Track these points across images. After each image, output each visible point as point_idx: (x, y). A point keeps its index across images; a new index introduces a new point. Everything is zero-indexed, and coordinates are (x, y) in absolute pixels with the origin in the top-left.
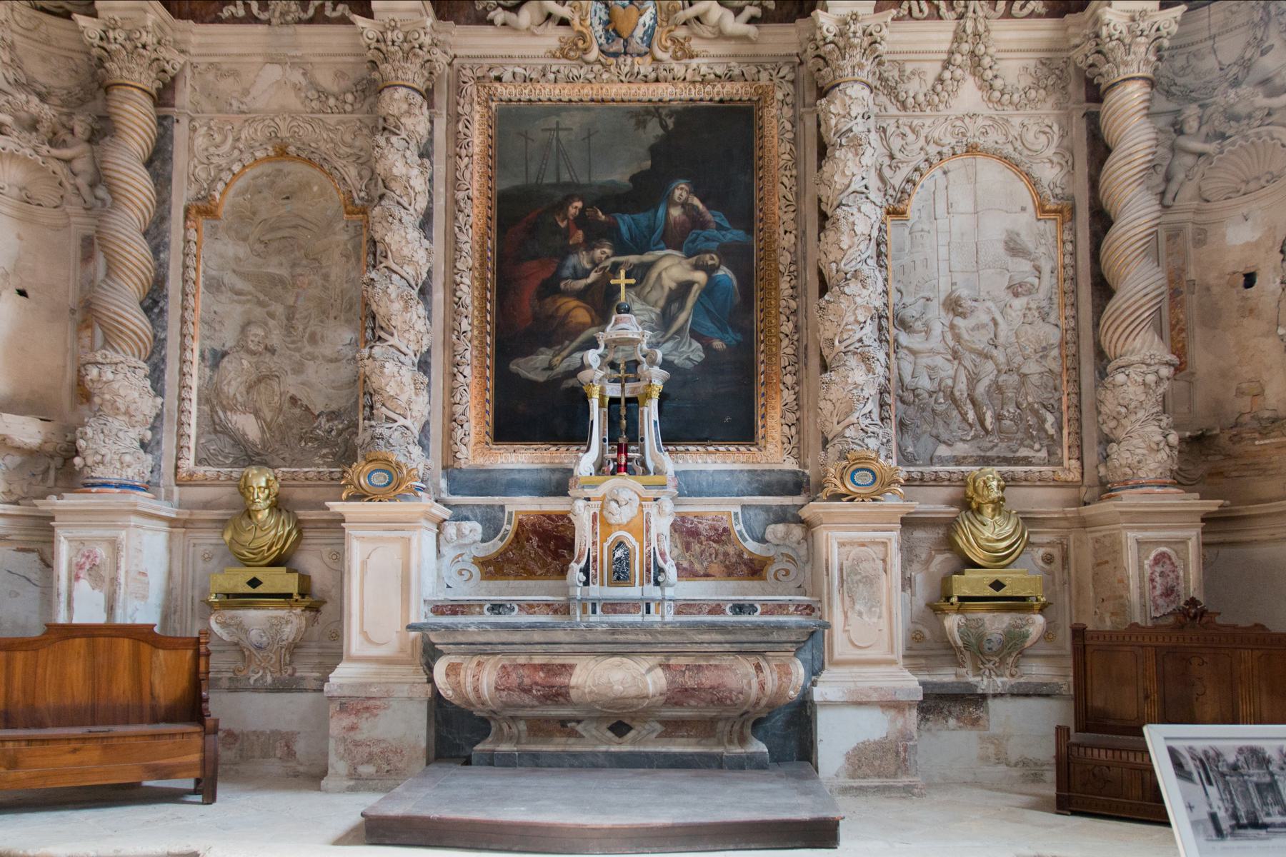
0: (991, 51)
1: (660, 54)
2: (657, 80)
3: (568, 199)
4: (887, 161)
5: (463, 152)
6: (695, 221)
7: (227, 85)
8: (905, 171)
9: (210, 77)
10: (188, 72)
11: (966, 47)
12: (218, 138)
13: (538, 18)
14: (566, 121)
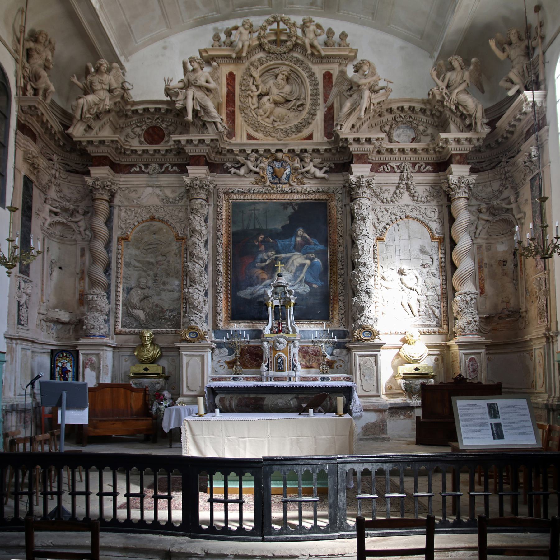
0: (414, 183)
1: (292, 183)
2: (291, 192)
3: (259, 234)
4: (377, 221)
5: (220, 218)
8: (383, 224)
10: (119, 191)
11: (404, 182)
13: (247, 171)
14: (258, 207)
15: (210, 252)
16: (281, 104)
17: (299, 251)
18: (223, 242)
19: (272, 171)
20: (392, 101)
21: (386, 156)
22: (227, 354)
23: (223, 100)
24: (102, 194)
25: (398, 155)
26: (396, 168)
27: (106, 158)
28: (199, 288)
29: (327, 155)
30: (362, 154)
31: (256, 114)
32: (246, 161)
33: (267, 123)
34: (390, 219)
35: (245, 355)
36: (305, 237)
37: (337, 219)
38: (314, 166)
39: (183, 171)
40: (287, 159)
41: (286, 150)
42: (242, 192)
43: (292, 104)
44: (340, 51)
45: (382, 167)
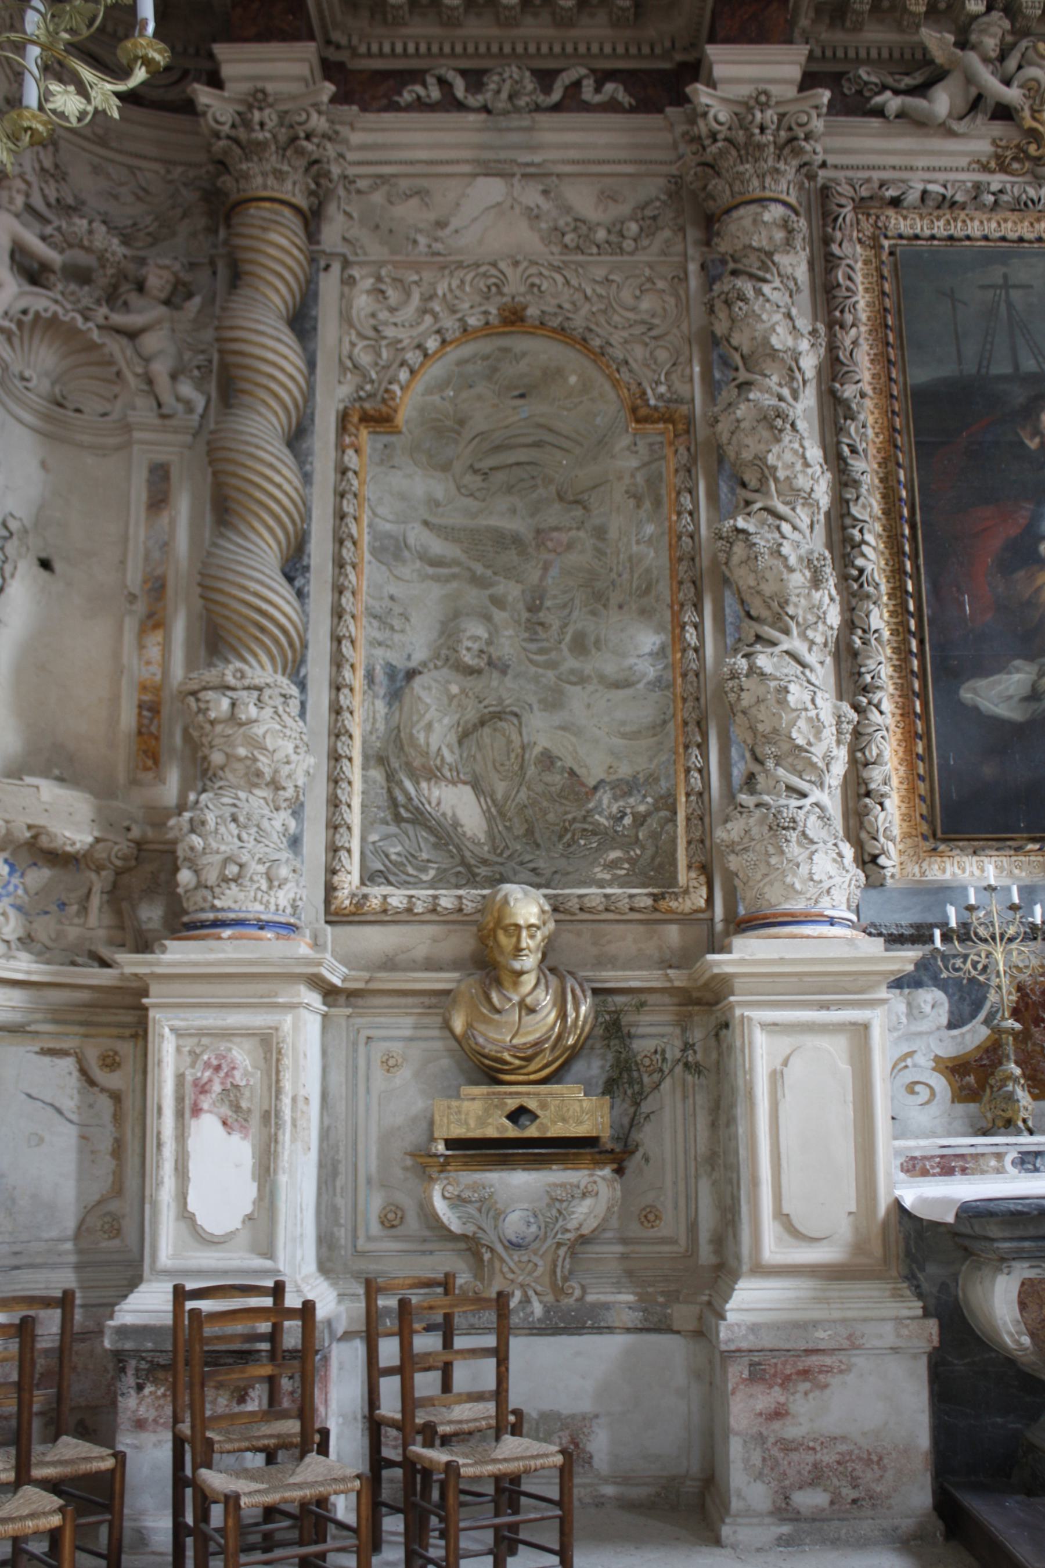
7: (408, 212)
9: (378, 197)
12: (393, 295)
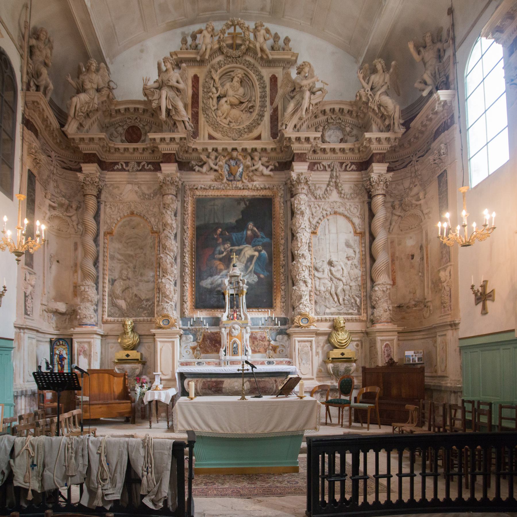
0: (341, 181)
1: (244, 181)
2: (243, 189)
6: (255, 235)
10: (105, 187)
14: (217, 202)
15: (178, 244)
16: (235, 105)
17: (250, 244)
18: (189, 235)
19: (229, 170)
20: (326, 103)
21: (320, 155)
22: (192, 340)
23: (189, 101)
24: (91, 190)
25: (329, 155)
26: (327, 167)
27: (94, 155)
28: (170, 278)
29: (273, 154)
30: (301, 153)
31: (216, 115)
32: (208, 159)
33: (225, 124)
34: (321, 215)
35: (206, 341)
36: (255, 231)
37: (280, 214)
38: (262, 164)
39: (157, 168)
40: (240, 158)
41: (239, 149)
42: (204, 189)
43: (244, 105)
44: (284, 54)
45: (316, 166)
